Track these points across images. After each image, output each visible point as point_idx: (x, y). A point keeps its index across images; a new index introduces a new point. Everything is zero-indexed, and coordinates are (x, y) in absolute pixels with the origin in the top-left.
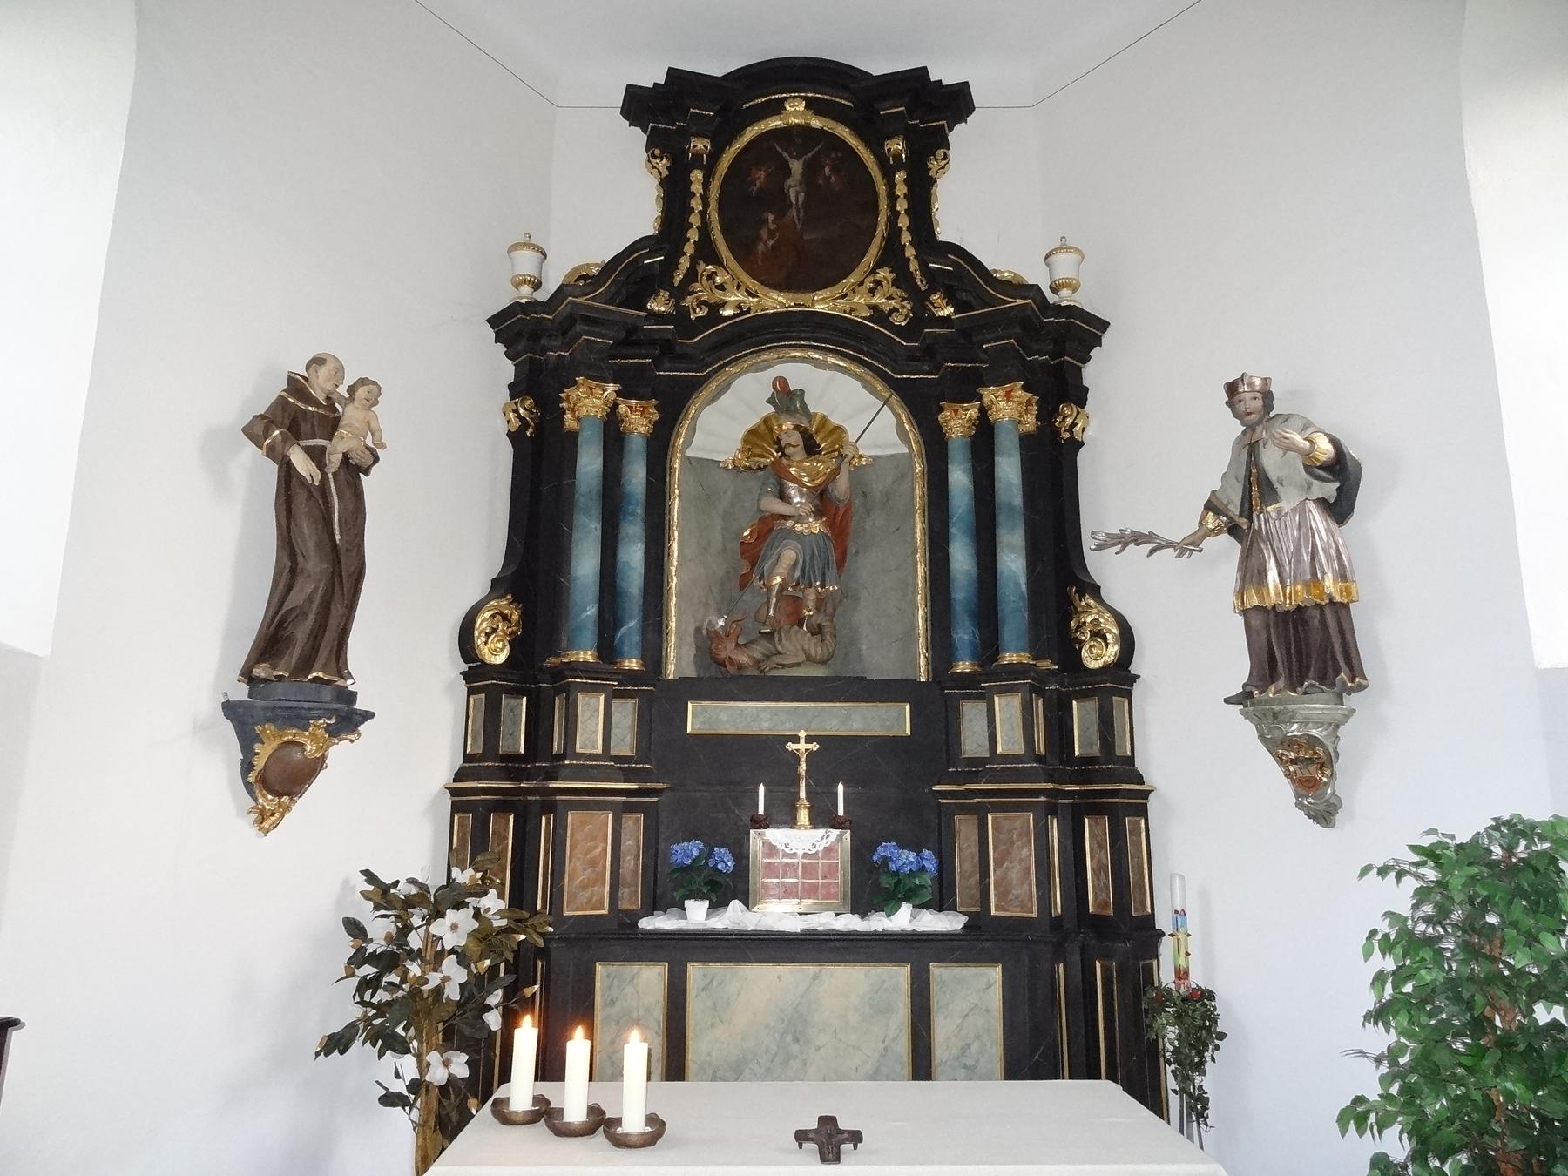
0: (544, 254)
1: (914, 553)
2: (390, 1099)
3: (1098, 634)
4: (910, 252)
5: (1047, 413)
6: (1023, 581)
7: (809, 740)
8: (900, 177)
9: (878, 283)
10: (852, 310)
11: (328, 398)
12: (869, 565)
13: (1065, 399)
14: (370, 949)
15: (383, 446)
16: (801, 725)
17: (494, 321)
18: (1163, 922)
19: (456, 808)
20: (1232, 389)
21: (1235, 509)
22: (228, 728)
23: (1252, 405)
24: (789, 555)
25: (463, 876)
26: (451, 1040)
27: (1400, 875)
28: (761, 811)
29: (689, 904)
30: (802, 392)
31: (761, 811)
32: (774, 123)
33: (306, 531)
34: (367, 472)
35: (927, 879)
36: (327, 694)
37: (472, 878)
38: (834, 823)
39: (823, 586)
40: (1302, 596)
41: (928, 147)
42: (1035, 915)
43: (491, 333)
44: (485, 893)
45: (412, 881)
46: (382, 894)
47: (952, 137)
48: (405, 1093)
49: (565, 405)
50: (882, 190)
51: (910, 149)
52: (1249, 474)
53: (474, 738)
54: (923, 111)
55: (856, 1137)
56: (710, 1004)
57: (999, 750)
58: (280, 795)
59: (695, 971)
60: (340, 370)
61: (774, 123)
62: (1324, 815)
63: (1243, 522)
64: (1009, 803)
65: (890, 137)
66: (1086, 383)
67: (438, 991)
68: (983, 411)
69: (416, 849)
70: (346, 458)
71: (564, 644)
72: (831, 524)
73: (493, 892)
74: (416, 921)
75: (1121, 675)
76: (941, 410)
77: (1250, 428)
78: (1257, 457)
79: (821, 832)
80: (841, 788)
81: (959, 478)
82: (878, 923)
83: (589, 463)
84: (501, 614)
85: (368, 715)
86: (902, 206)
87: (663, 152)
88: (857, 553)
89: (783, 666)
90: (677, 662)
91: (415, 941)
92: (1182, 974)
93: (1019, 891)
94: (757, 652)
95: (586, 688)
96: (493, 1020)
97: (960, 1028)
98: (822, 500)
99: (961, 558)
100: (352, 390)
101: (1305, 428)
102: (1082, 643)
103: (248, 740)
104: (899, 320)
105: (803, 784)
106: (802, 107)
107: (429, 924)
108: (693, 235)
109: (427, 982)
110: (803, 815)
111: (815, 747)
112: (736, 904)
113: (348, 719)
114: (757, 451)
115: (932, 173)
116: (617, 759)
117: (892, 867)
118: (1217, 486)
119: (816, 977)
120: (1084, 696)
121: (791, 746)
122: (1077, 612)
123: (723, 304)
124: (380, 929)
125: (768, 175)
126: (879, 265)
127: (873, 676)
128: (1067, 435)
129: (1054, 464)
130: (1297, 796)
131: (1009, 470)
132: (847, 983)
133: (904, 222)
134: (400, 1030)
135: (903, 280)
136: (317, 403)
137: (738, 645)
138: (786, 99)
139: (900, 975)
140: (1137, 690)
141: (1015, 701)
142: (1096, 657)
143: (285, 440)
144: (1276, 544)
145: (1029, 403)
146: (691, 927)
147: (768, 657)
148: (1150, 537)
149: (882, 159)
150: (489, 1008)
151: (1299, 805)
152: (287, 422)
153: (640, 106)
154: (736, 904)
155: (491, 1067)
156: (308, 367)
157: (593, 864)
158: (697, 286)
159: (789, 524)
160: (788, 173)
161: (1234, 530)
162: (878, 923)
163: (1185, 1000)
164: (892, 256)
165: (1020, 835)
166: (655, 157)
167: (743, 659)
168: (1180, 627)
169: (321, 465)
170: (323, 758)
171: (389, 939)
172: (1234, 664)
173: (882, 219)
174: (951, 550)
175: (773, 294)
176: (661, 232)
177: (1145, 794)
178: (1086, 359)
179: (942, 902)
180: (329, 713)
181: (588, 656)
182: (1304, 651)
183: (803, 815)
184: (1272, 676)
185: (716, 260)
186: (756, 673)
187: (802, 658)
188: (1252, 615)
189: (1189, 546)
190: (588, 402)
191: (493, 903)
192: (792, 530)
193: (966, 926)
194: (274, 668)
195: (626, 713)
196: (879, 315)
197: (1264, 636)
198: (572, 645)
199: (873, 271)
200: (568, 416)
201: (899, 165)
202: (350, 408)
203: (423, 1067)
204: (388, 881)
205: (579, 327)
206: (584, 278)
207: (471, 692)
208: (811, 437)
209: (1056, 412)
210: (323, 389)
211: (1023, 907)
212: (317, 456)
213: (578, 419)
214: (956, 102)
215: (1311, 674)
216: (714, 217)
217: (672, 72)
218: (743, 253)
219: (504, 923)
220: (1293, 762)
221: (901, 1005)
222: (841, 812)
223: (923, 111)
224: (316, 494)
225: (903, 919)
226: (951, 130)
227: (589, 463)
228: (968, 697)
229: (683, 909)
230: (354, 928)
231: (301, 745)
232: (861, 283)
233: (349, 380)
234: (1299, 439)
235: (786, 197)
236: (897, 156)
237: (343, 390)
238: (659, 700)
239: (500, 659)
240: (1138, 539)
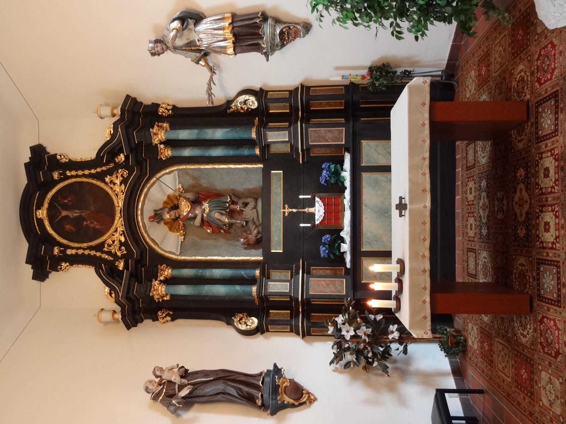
0: (102, 310)
1: (215, 168)
2: (405, 351)
3: (245, 102)
4: (99, 170)
5: (161, 119)
6: (226, 130)
7: (284, 208)
8: (68, 173)
9: (111, 182)
10: (122, 191)
11: (160, 385)
12: (220, 185)
13: (157, 112)
14: (355, 360)
15: (178, 365)
16: (279, 211)
17: (128, 328)
18: (347, 82)
19: (309, 334)
20: (153, 54)
21: (198, 55)
22: (279, 413)
23: (160, 46)
24: (217, 215)
25: (331, 329)
26: (386, 332)
27: (322, 16)
28: (309, 225)
29: (342, 251)
30: (155, 211)
31: (309, 225)
32: (46, 223)
33: (210, 390)
34: (188, 370)
35: (332, 167)
36: (267, 380)
37: (332, 326)
38: (313, 199)
39: (228, 203)
41: (54, 162)
42: (344, 129)
43: (133, 329)
44: (336, 322)
45: (333, 348)
46: (338, 357)
47: (52, 153)
48: (403, 346)
49: (160, 300)
50: (74, 180)
51: (57, 169)
52: (186, 50)
53: (285, 328)
54: (41, 163)
55: (401, 198)
56: (375, 242)
57: (287, 140)
58: (303, 394)
59: (365, 248)
60: (151, 382)
61: (46, 223)
62: (307, 27)
63: (202, 53)
64: (305, 137)
65: (52, 177)
66: (150, 103)
67: (368, 336)
68: (161, 143)
69: (324, 349)
70: (182, 377)
71: (250, 298)
72: (205, 200)
73: (336, 319)
74: (347, 346)
75: (259, 94)
76: (161, 158)
77: (168, 48)
78: (179, 47)
79: (316, 204)
80: (301, 197)
81: (187, 152)
82: (348, 184)
83: (183, 290)
84: (239, 321)
85: (275, 365)
86: (80, 173)
87: (59, 265)
88: (216, 190)
89: (258, 217)
90: (256, 256)
91: (353, 346)
92: (363, 77)
93: (336, 134)
94: (252, 227)
95: (266, 289)
96: (379, 317)
97: (382, 155)
98: (196, 202)
99: (217, 152)
100: (157, 377)
101: (168, 30)
102: (248, 108)
103: (284, 406)
104: (126, 173)
105: (300, 210)
106: (40, 211)
107: (348, 341)
108: (93, 253)
109: (365, 340)
110: (311, 210)
111: (286, 206)
112: (342, 234)
113: (277, 371)
114: (177, 227)
115: (67, 161)
116: (292, 277)
117: (328, 178)
118: (189, 59)
119: (366, 206)
120: (267, 109)
121: (286, 214)
122: (237, 109)
123: (120, 241)
124: (349, 357)
125: (67, 224)
126: (104, 181)
127: (261, 183)
129: (183, 116)
130: (300, 37)
131: (184, 134)
132: (368, 196)
133: (87, 172)
134: (381, 349)
135: (110, 172)
136: (162, 389)
137: (251, 234)
138: (36, 218)
139: (365, 176)
140: (265, 89)
141: (269, 134)
142: (253, 103)
143: (177, 398)
144: (211, 42)
145: (158, 126)
146: (349, 250)
147: (254, 223)
148: (209, 85)
149: (61, 180)
150: (375, 319)
151: (304, 36)
152: (169, 399)
153: (40, 274)
154: (342, 234)
155: (390, 316)
156: (149, 393)
157: (328, 285)
158: (113, 251)
159: (205, 215)
160: (67, 216)
161: (206, 54)
162: (348, 184)
163: (372, 77)
164: (100, 177)
165: (317, 133)
166: (61, 268)
167: (256, 231)
168: (242, 75)
169: (186, 386)
170: (290, 380)
171: (351, 354)
172: (254, 58)
173: (84, 180)
174: (214, 155)
175: (116, 222)
176: (93, 266)
177: (302, 86)
178: (141, 103)
179: (341, 162)
180: (274, 378)
181: (254, 289)
182: (248, 33)
183: (311, 210)
184: (258, 45)
185: (103, 243)
186: (260, 227)
187: (255, 210)
188: (236, 51)
190: (159, 290)
191: (340, 319)
192: (208, 214)
193: (348, 152)
194: (258, 398)
195: (275, 274)
196: (124, 181)
197: (245, 47)
198: (250, 294)
199: (107, 184)
200: (165, 299)
201: (64, 174)
202: (164, 377)
203: (394, 341)
204: (333, 356)
205: (131, 295)
206: (110, 294)
207: (268, 331)
208: (172, 207)
209: (161, 116)
210: (157, 387)
211: (341, 132)
212: (181, 387)
213: (167, 295)
214: (38, 151)
215: (257, 32)
216: (85, 245)
217: (27, 262)
218: (99, 233)
219: (347, 315)
220: (289, 38)
221: (375, 175)
222: (309, 197)
223: (41, 163)
224: (196, 387)
225: (346, 175)
226: (49, 153)
227: (183, 290)
228: (268, 151)
229: (344, 252)
230: (347, 365)
231: (286, 387)
232: (111, 188)
233: (153, 378)
234: (173, 34)
235: (76, 218)
236: (60, 174)
237: (157, 380)
238: (270, 264)
239: (255, 320)
240: (210, 88)
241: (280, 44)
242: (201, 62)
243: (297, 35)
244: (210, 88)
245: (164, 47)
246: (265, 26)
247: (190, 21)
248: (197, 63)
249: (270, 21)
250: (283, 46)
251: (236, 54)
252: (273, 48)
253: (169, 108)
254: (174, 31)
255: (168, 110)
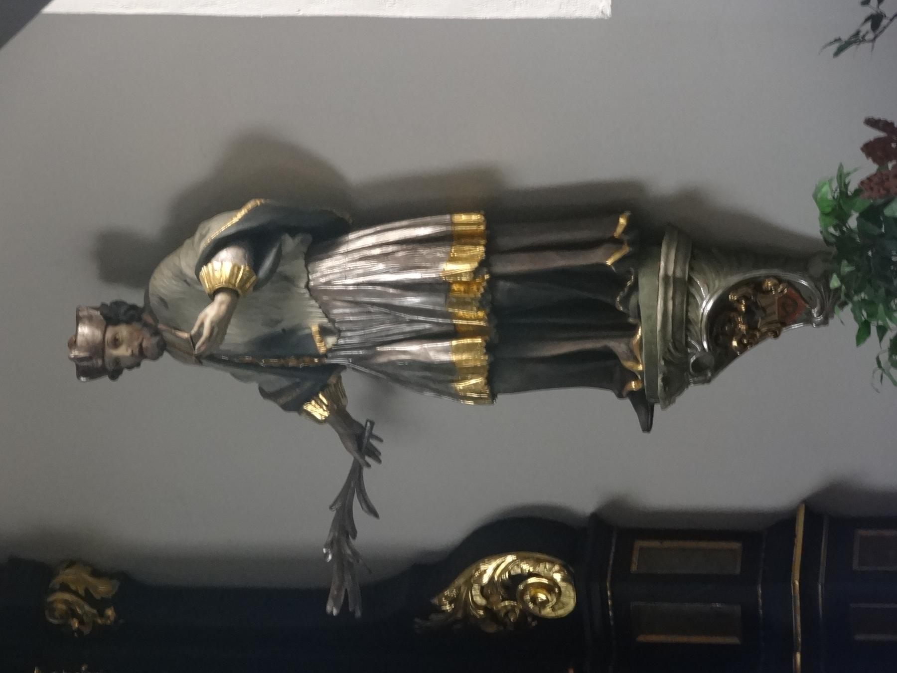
3: (512, 585)
40: (472, 317)
77: (163, 347)
102: (525, 613)
122: (467, 616)
128: (110, 612)
142: (551, 589)
189: (361, 441)
234: (211, 312)
240: (344, 527)
241: (709, 360)
242: (311, 407)
243: (791, 311)
244: (344, 527)
245: (149, 342)
246: (644, 282)
247: (290, 243)
248: (296, 406)
249: (668, 262)
250: (723, 357)
251: (493, 396)
252: (682, 370)
253: (103, 588)
254: (220, 298)
255: (100, 605)
